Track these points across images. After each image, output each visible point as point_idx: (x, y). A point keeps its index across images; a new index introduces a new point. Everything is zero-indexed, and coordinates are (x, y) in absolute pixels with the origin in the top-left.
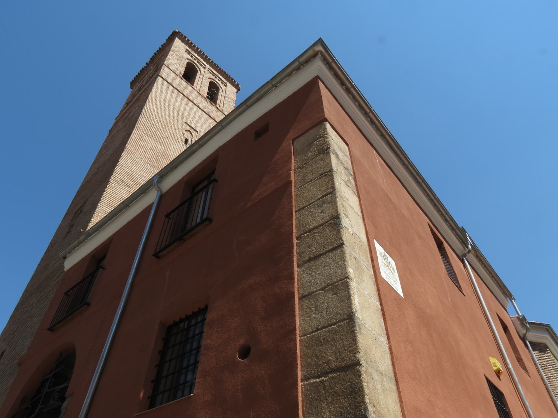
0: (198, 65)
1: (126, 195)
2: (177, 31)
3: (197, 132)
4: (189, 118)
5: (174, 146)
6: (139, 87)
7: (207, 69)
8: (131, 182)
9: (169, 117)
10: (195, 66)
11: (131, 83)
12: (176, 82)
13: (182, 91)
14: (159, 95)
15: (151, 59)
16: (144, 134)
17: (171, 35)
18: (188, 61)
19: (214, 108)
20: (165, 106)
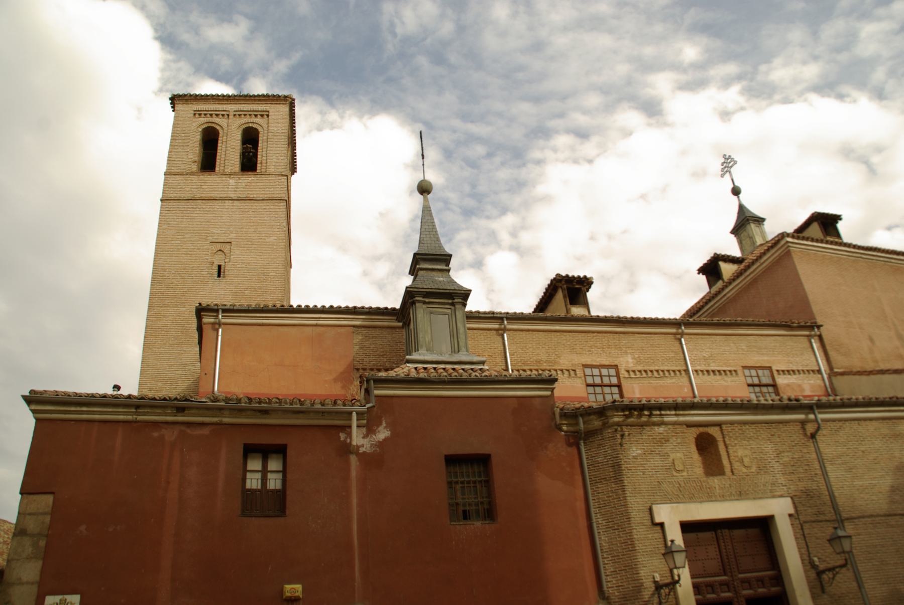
0: (217, 120)
3: (230, 242)
4: (214, 231)
5: (201, 293)
8: (160, 384)
13: (197, 197)
14: (167, 232)
16: (161, 307)
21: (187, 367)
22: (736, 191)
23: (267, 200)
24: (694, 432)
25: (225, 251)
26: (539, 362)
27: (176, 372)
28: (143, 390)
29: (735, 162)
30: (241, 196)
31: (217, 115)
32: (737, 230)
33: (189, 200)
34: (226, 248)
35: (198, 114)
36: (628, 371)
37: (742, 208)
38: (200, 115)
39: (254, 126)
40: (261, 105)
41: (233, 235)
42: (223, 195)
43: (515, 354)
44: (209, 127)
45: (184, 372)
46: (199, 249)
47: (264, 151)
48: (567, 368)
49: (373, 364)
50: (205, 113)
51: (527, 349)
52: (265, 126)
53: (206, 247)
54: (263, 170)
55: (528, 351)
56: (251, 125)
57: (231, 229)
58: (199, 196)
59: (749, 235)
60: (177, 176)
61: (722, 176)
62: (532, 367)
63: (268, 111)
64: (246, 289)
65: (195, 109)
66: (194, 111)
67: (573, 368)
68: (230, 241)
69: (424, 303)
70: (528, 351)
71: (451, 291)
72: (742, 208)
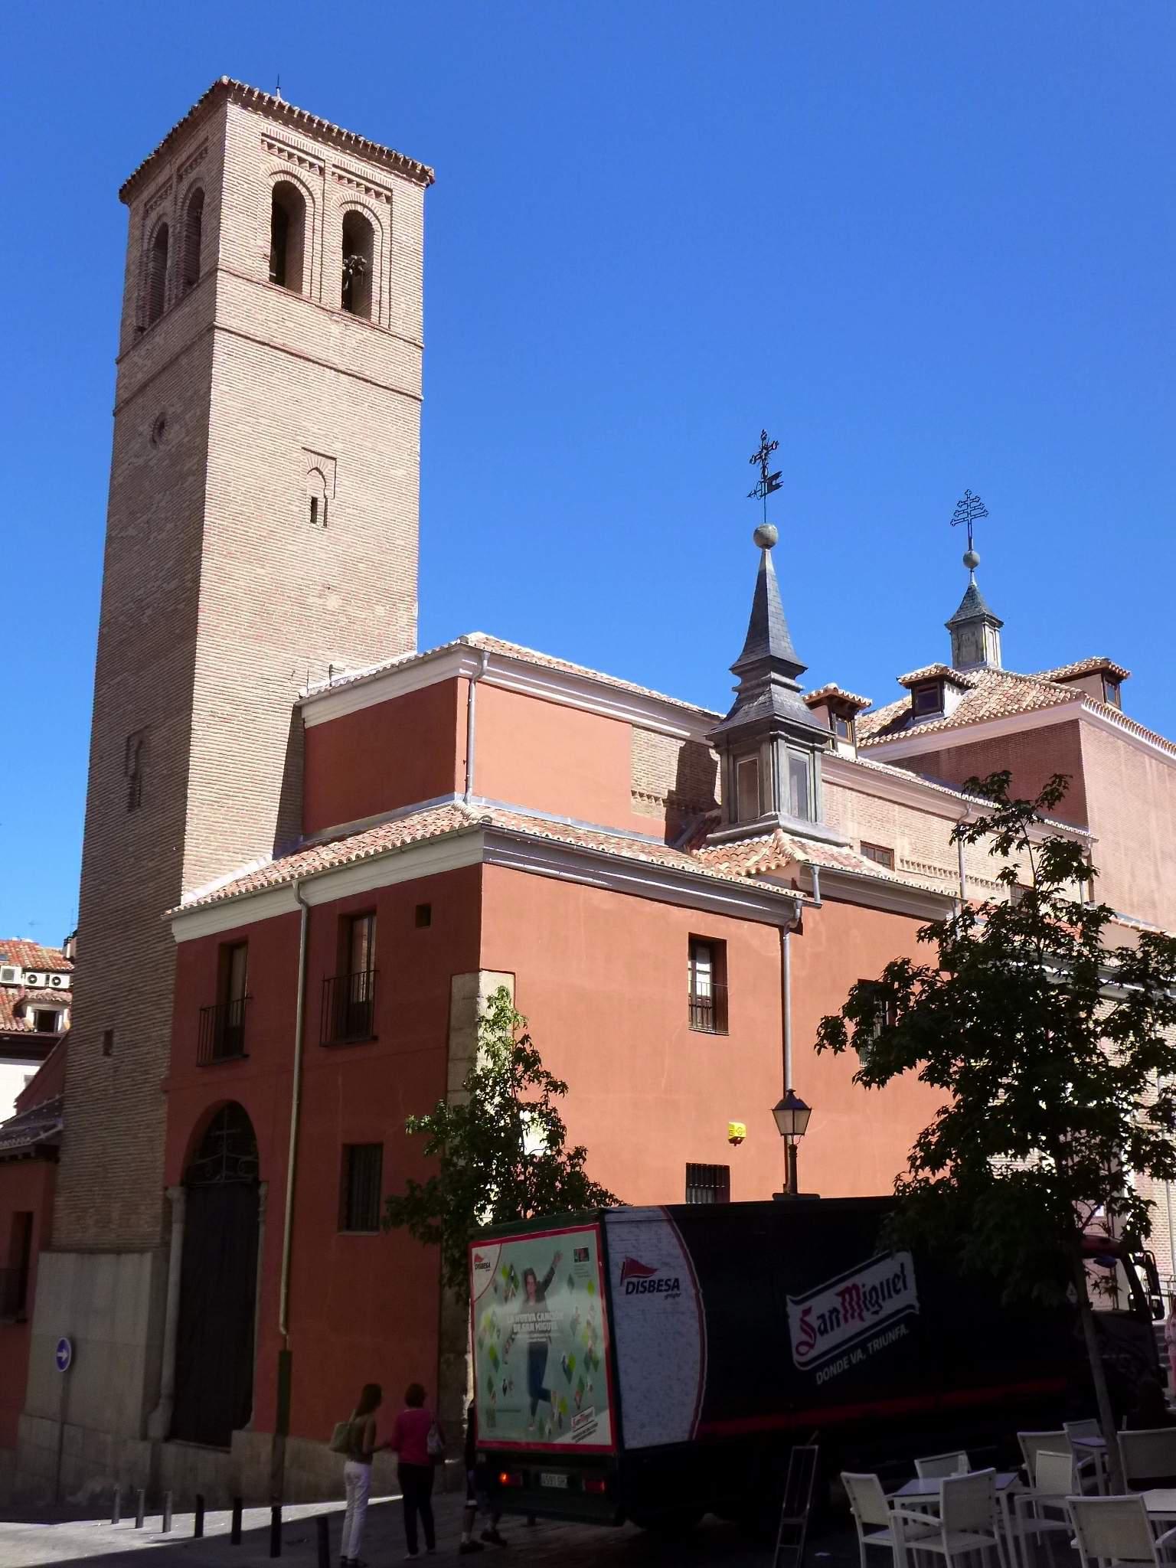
0: (303, 173)
1: (227, 744)
2: (225, 80)
3: (334, 459)
5: (290, 547)
6: (150, 239)
7: (329, 170)
8: (228, 707)
9: (264, 460)
10: (295, 188)
11: (121, 191)
12: (259, 317)
13: (278, 342)
15: (166, 141)
17: (212, 91)
19: (367, 333)
20: (250, 430)
21: (271, 686)
22: (969, 562)
23: (393, 390)
25: (324, 473)
27: (254, 690)
28: (202, 713)
29: (985, 513)
30: (351, 367)
32: (958, 627)
34: (327, 467)
35: (270, 143)
36: (902, 861)
37: (971, 593)
39: (364, 213)
40: (379, 171)
41: (338, 446)
44: (286, 182)
45: (267, 693)
46: (283, 456)
47: (386, 279)
49: (652, 789)
52: (386, 222)
53: (295, 455)
54: (385, 323)
56: (359, 208)
57: (336, 430)
58: (281, 342)
59: (976, 642)
60: (240, 280)
61: (953, 523)
63: (390, 190)
64: (361, 560)
68: (334, 456)
69: (788, 741)
72: (971, 593)
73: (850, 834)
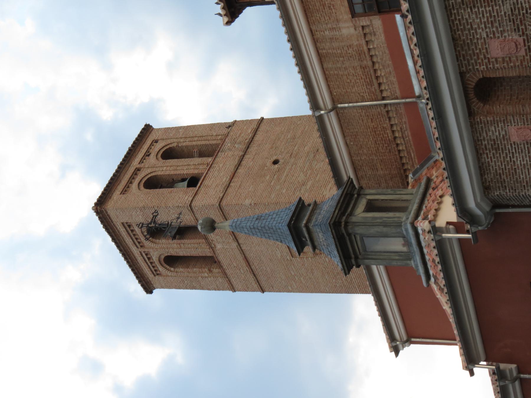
18: (172, 269)
24: (477, 105)
26: (363, 68)
31: (149, 259)
33: (257, 281)
38: (155, 270)
42: (237, 252)
43: (362, 94)
48: (363, 36)
50: (152, 268)
51: (351, 81)
55: (353, 81)
62: (373, 77)
65: (153, 275)
66: (155, 276)
67: (361, 29)
70: (353, 81)
71: (337, 240)
73: (352, 30)
